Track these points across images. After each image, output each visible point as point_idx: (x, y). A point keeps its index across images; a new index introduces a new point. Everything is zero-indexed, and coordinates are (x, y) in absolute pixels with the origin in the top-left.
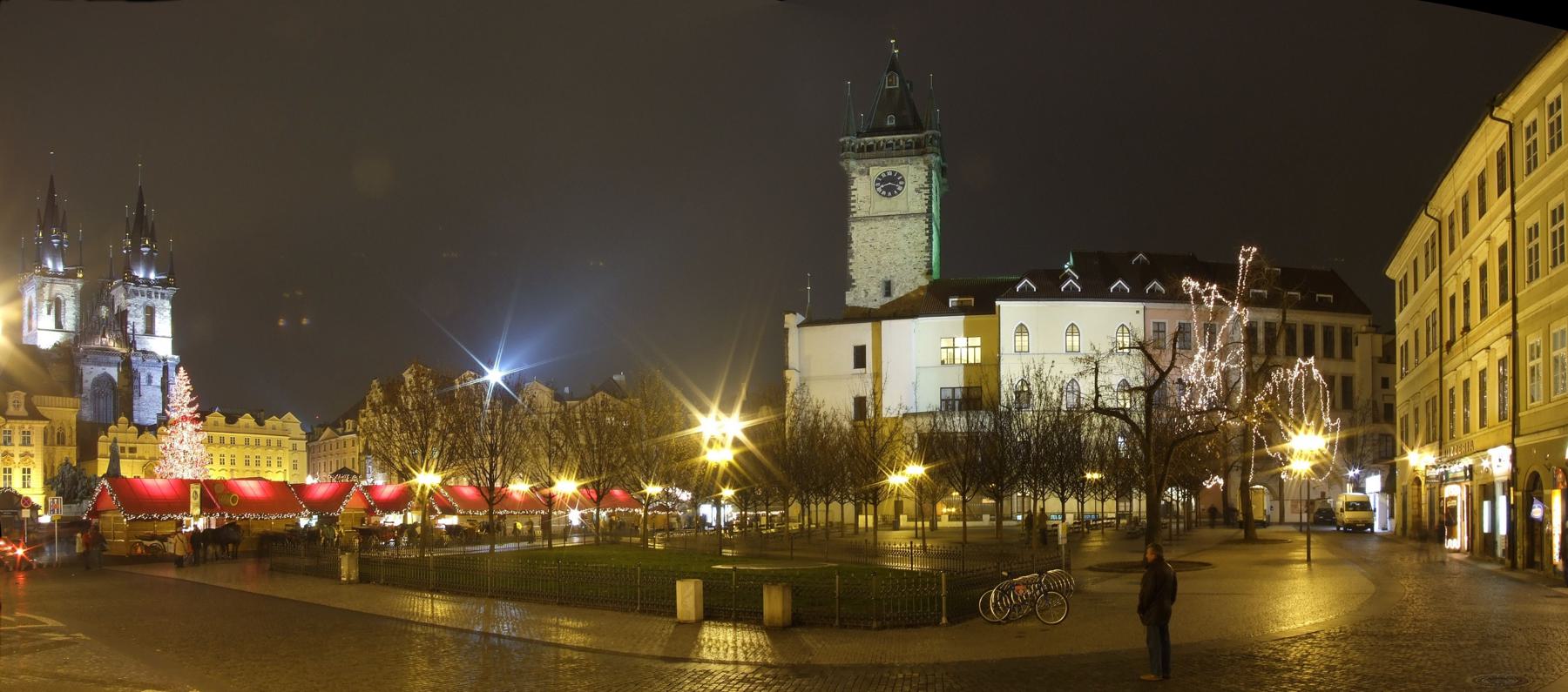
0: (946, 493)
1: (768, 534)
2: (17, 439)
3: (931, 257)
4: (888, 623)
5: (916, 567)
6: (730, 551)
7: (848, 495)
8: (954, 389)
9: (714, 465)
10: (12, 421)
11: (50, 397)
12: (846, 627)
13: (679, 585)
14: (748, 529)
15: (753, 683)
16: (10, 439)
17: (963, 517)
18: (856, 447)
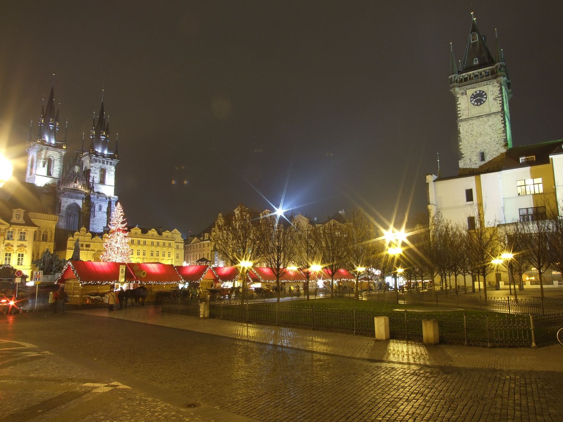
0: (527, 268)
1: (423, 292)
2: (16, 236)
3: (506, 136)
4: (497, 344)
5: (512, 312)
6: (403, 302)
7: (467, 270)
8: (527, 209)
9: (392, 256)
10: (13, 226)
11: (40, 214)
12: (471, 345)
13: (376, 320)
14: (412, 290)
15: (419, 376)
16: (12, 236)
17: (541, 282)
18: (471, 244)
